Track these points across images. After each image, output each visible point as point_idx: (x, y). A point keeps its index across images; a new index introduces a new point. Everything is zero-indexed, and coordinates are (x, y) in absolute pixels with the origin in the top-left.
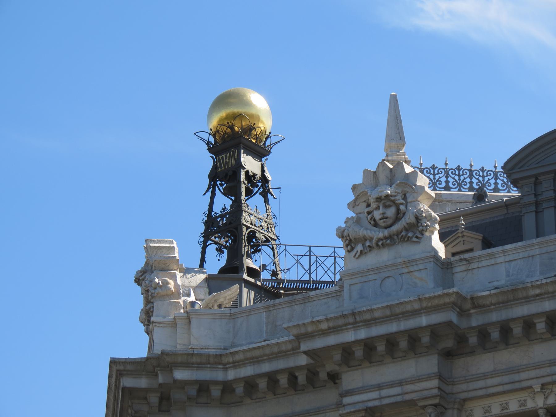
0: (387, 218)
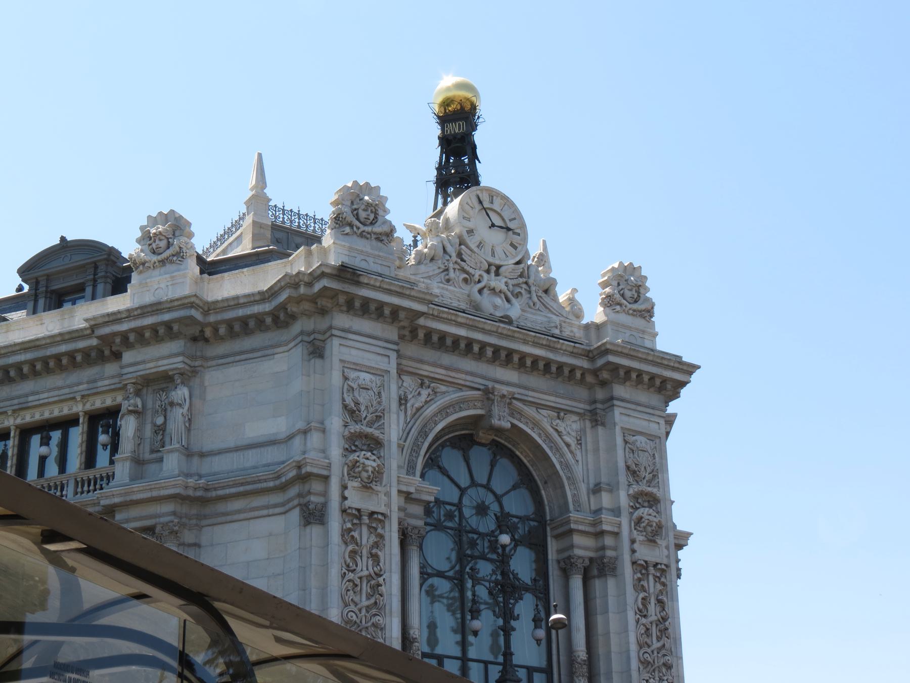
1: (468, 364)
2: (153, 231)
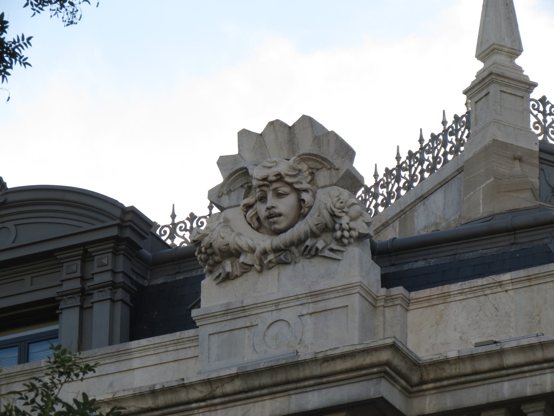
0: (280, 215)
2: (257, 173)
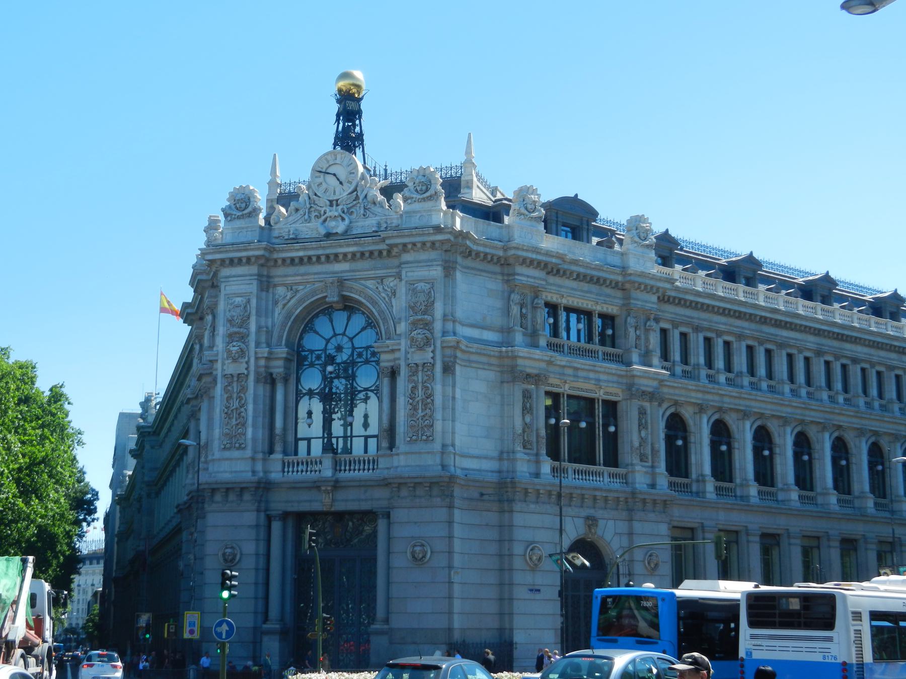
1: (317, 268)
